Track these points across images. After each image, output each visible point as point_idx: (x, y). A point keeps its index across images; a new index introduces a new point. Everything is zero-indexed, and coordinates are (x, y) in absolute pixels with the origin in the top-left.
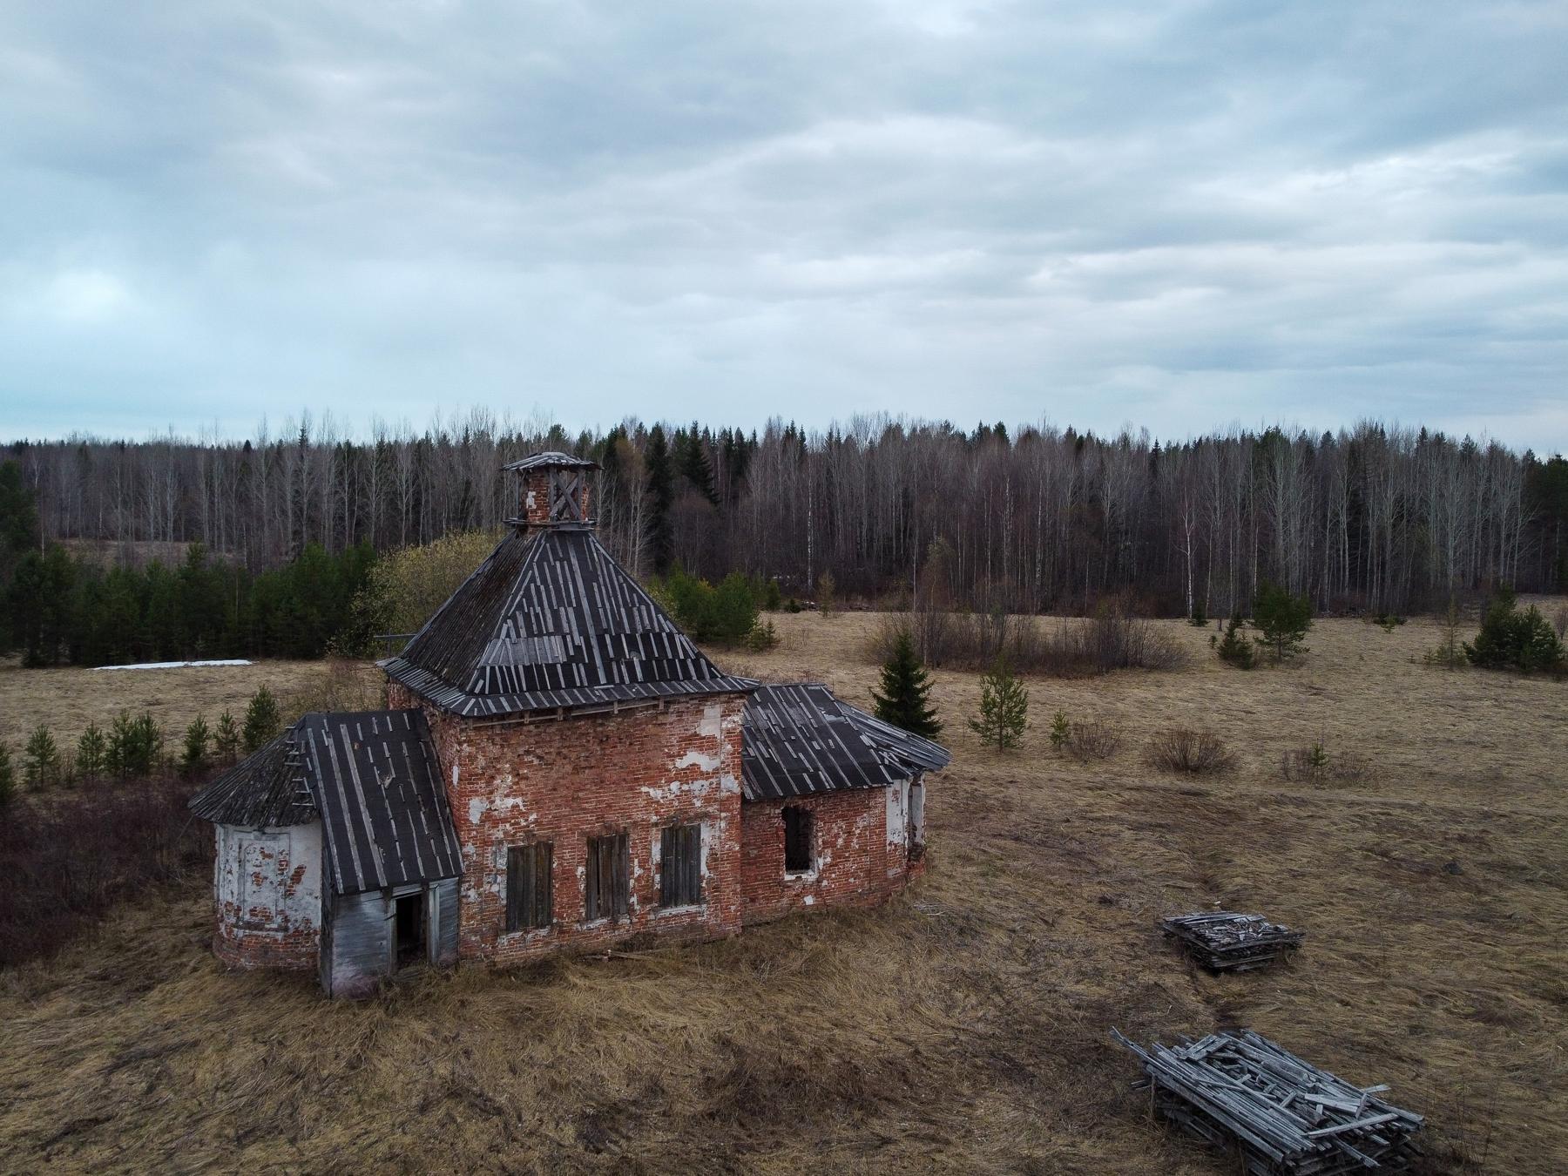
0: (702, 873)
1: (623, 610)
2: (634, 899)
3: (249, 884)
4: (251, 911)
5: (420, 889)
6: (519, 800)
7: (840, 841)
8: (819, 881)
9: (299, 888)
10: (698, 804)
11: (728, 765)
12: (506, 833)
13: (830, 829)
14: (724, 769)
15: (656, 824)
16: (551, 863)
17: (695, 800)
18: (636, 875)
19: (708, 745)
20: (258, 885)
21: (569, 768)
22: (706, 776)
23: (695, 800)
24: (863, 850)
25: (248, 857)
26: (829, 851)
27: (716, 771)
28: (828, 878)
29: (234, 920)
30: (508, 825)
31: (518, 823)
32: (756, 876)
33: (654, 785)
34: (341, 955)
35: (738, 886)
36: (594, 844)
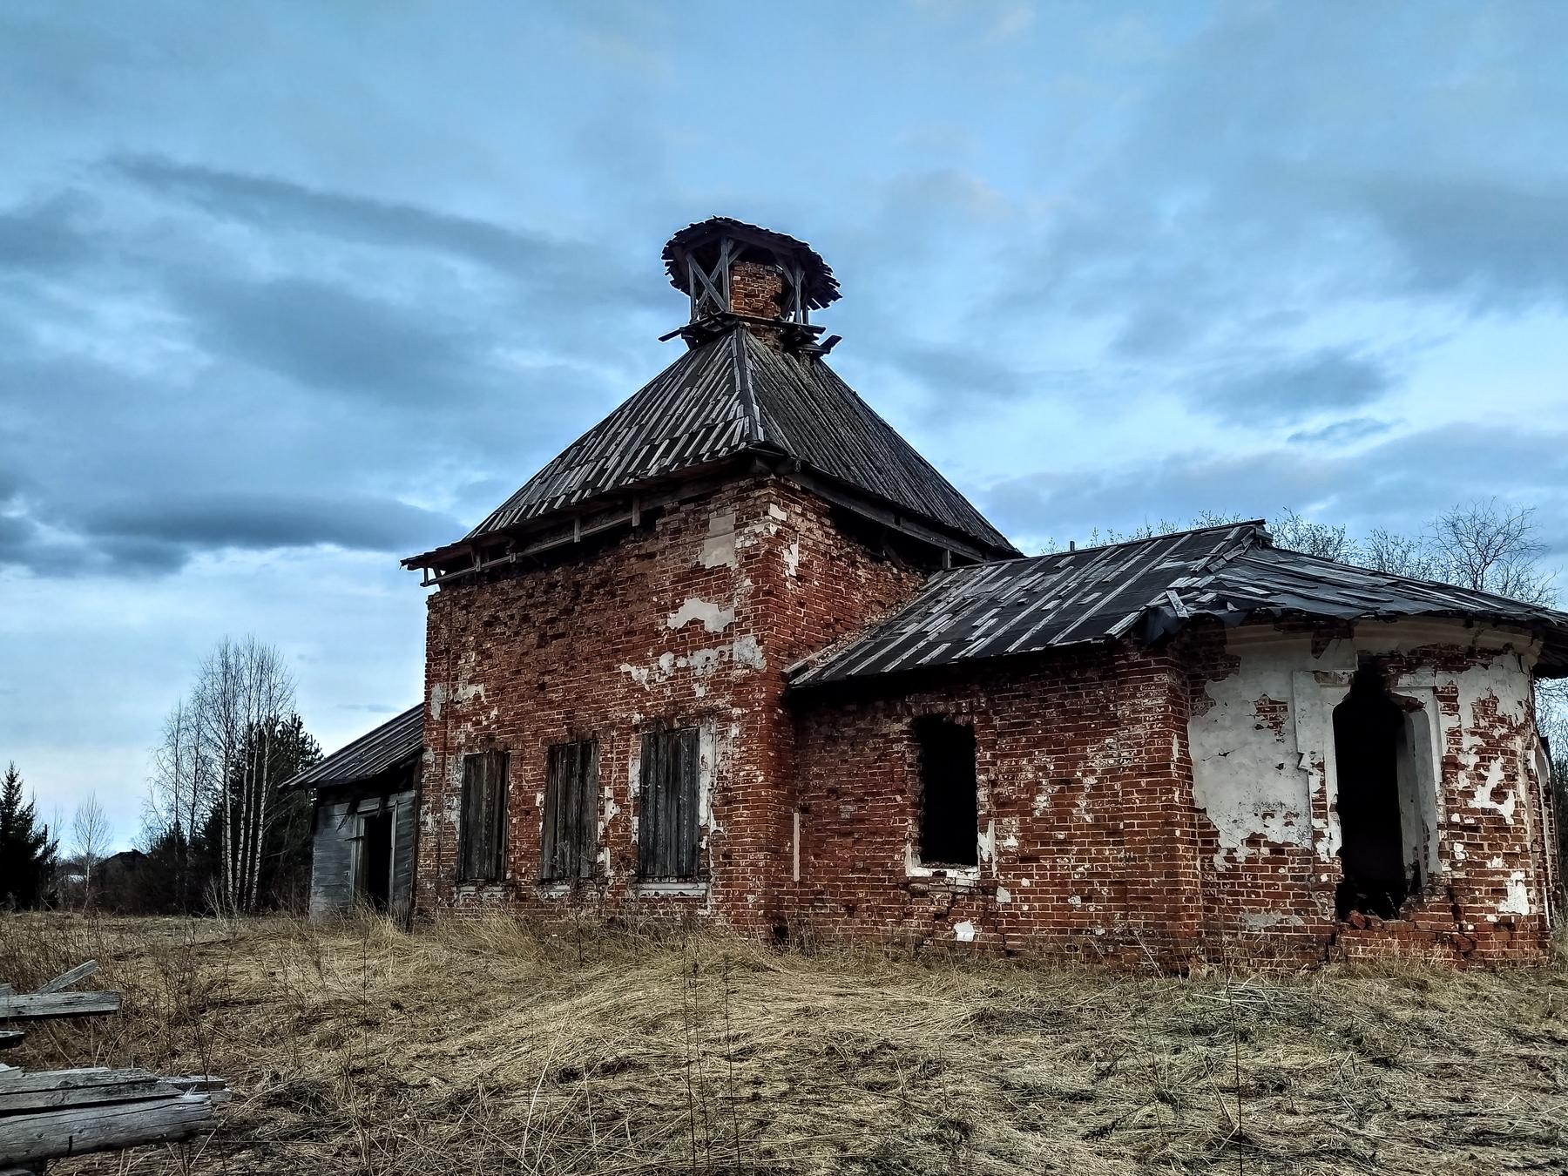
0: (702, 822)
1: (695, 410)
2: (605, 857)
6: (481, 688)
7: (1041, 802)
8: (986, 888)
10: (700, 692)
11: (747, 618)
12: (468, 736)
13: (1014, 773)
14: (739, 625)
15: (636, 728)
16: (504, 783)
17: (696, 686)
18: (609, 816)
19: (714, 583)
21: (533, 638)
22: (712, 640)
23: (696, 686)
24: (1108, 829)
26: (1014, 822)
27: (728, 633)
28: (1012, 888)
31: (479, 723)
32: (854, 858)
33: (641, 661)
34: (318, 882)
35: (761, 855)
36: (554, 752)
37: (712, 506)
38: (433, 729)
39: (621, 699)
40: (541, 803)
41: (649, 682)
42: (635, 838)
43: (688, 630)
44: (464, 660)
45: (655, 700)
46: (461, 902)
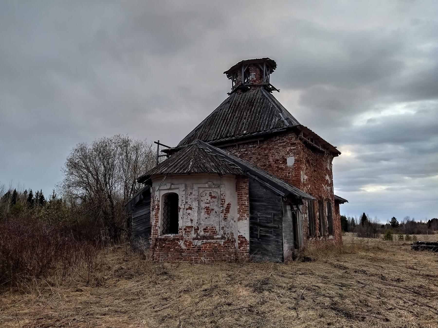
3: (202, 214)
4: (204, 229)
9: (229, 215)
20: (208, 214)
25: (202, 199)
29: (195, 236)
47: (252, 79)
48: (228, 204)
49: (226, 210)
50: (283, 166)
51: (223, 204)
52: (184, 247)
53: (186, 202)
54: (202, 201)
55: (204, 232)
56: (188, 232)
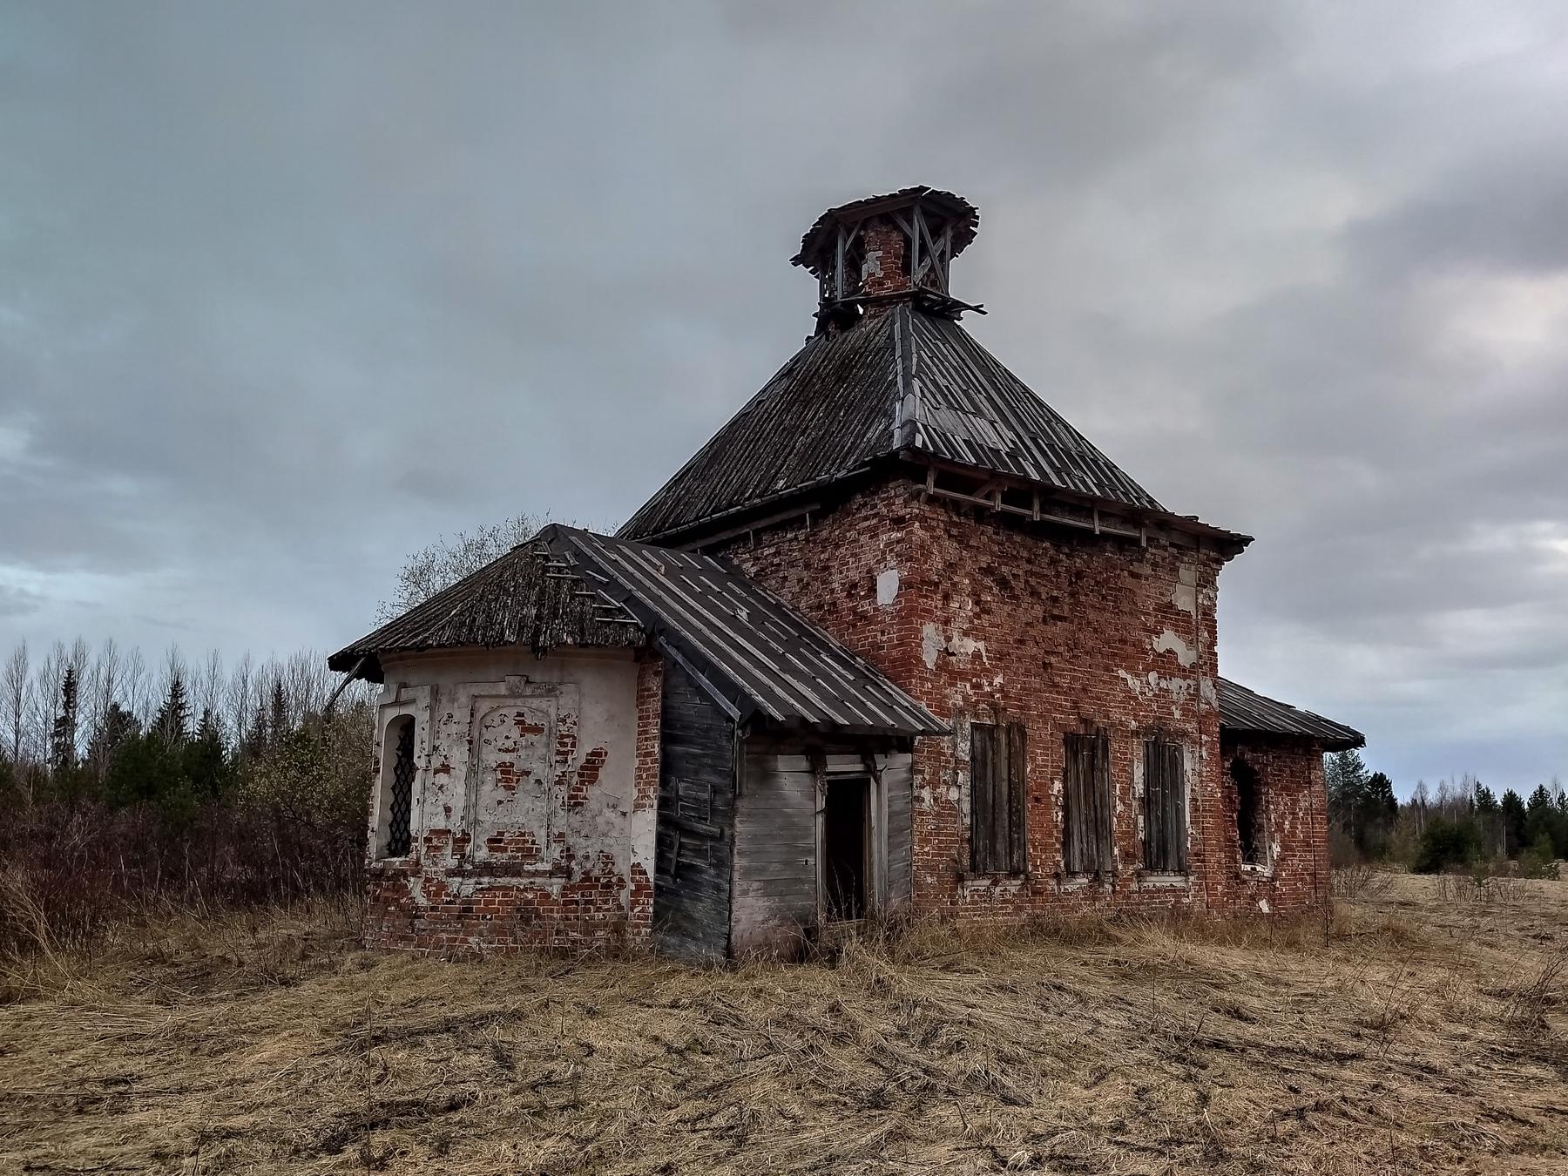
1: (1040, 420)
3: (487, 788)
4: (491, 841)
5: (859, 767)
6: (981, 645)
9: (593, 792)
10: (1177, 714)
12: (965, 698)
15: (1136, 734)
17: (1174, 708)
20: (508, 788)
21: (1038, 611)
23: (1174, 708)
29: (452, 862)
30: (968, 685)
34: (747, 873)
36: (1072, 743)
37: (1186, 559)
38: (927, 680)
39: (1120, 702)
40: (1059, 791)
41: (1141, 693)
42: (1141, 835)
43: (1165, 657)
44: (957, 605)
45: (1146, 711)
46: (968, 899)
47: (870, 275)
48: (595, 753)
49: (580, 775)
50: (865, 606)
51: (566, 753)
52: (422, 901)
53: (435, 748)
54: (487, 742)
55: (491, 849)
56: (437, 848)
